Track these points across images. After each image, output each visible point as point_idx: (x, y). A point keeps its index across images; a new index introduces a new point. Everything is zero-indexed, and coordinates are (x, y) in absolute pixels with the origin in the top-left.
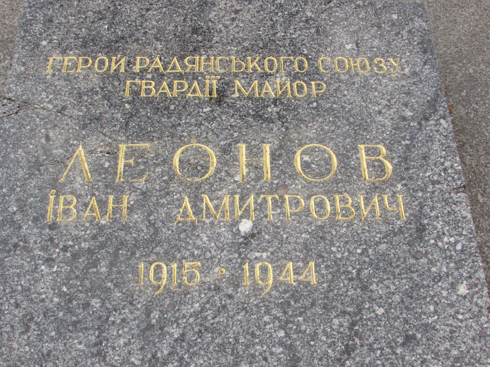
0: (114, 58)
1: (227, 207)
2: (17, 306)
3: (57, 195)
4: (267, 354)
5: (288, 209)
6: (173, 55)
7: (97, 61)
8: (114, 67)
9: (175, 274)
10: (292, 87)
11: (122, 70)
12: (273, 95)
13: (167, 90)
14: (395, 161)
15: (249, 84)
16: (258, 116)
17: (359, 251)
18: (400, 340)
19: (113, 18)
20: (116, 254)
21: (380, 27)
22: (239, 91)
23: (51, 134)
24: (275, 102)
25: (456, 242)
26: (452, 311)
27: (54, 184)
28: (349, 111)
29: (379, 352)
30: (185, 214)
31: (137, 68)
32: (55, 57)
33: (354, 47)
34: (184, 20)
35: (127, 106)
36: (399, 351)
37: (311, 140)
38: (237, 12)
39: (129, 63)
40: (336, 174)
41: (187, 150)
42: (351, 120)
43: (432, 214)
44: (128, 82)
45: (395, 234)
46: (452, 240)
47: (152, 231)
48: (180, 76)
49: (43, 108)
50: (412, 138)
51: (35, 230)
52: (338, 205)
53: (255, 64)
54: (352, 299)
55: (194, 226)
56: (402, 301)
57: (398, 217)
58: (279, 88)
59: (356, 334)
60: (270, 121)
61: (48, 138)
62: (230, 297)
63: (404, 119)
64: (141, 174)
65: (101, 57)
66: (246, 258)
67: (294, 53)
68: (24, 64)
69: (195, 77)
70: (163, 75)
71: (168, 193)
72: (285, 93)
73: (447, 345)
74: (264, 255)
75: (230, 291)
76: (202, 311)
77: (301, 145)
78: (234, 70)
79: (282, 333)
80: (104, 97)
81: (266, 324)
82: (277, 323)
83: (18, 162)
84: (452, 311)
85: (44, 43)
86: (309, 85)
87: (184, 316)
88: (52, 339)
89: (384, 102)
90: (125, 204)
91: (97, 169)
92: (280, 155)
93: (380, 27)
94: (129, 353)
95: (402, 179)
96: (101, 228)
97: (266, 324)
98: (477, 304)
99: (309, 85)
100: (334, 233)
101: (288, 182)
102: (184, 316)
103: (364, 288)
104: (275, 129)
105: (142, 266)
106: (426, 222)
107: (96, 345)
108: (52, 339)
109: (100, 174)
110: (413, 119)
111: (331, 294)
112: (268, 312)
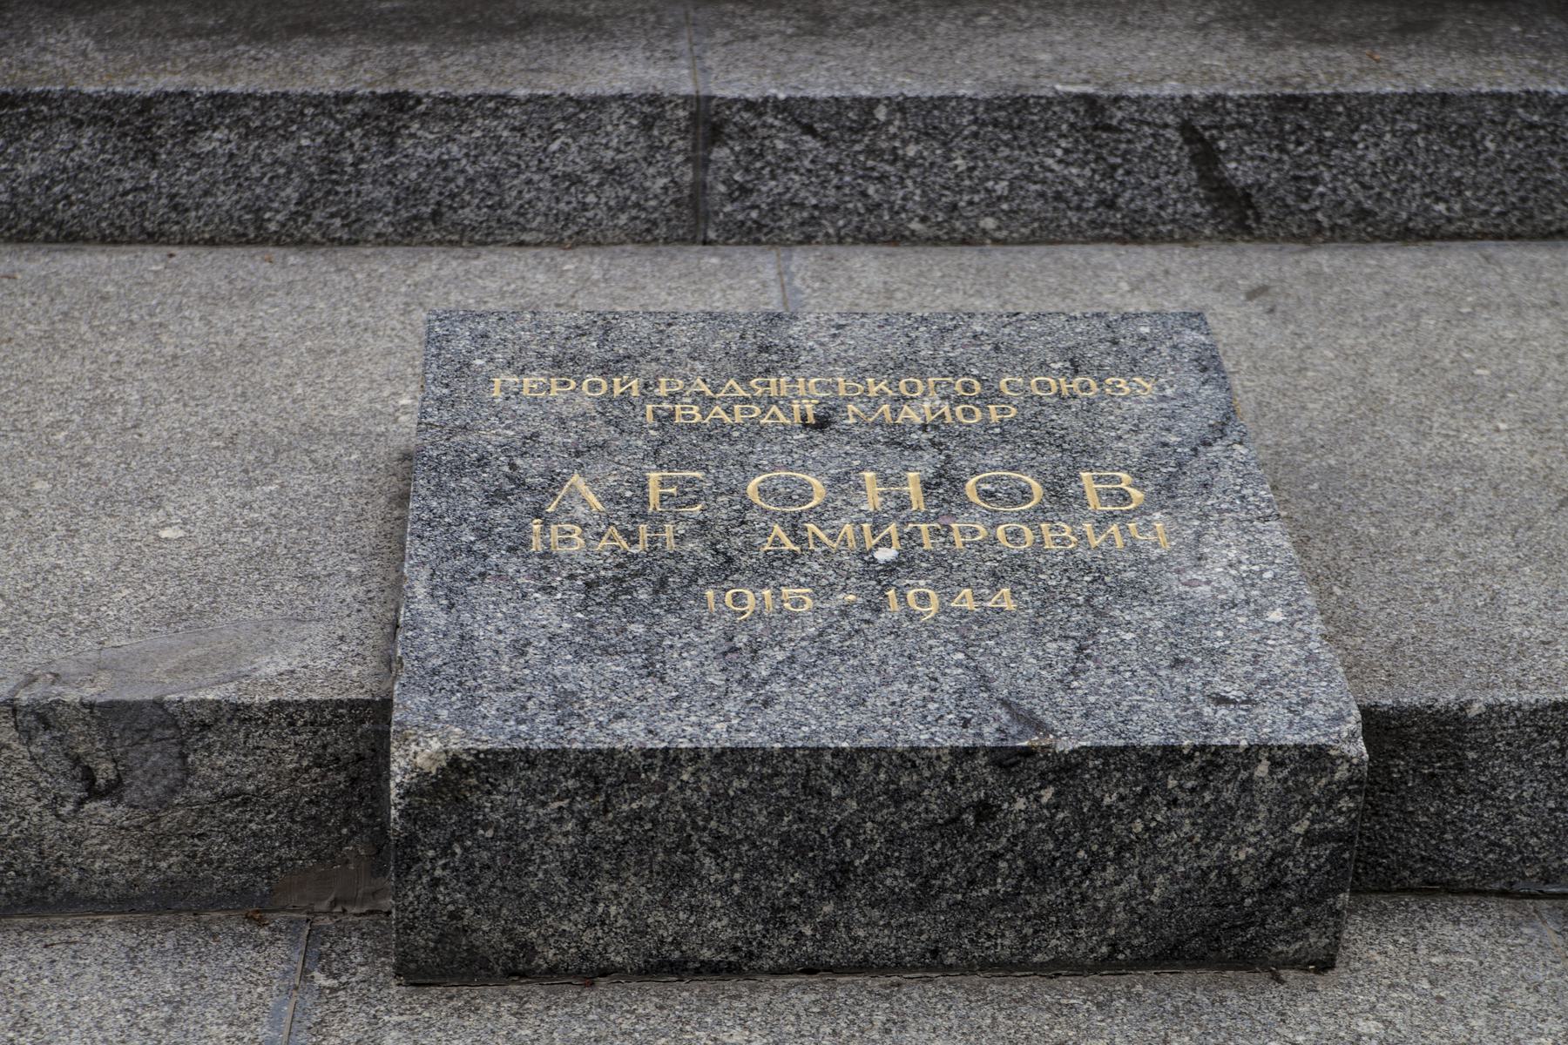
0: (616, 380)
1: (850, 536)
2: (500, 632)
3: (546, 524)
4: (938, 675)
5: (959, 541)
6: (728, 377)
7: (585, 383)
8: (618, 391)
9: (769, 602)
10: (953, 413)
11: (635, 393)
12: (919, 421)
13: (723, 415)
14: (1150, 489)
15: (874, 409)
16: (891, 443)
17: (1087, 578)
18: (1165, 663)
19: (606, 333)
20: (663, 583)
21: (1115, 342)
22: (856, 416)
23: (519, 462)
24: (924, 428)
25: (1262, 572)
26: (1257, 637)
27: (538, 513)
28: (1062, 437)
29: (1128, 674)
30: (776, 542)
31: (662, 391)
32: (504, 380)
33: (1068, 364)
34: (742, 337)
35: (652, 432)
36: (1163, 673)
37: (995, 468)
38: (840, 327)
39: (646, 386)
40: (1041, 502)
41: (770, 479)
42: (1066, 446)
43: (1221, 542)
44: (649, 407)
45: (1152, 563)
46: (1256, 568)
47: (721, 559)
48: (746, 400)
49: (497, 434)
50: (1179, 465)
51: (514, 559)
52: (1048, 536)
53: (881, 385)
54: (1079, 625)
55: (795, 555)
56: (1167, 627)
57: (1156, 545)
58: (928, 413)
59: (1088, 656)
60: (916, 448)
61: (513, 466)
62: (868, 622)
63: (1165, 445)
64: (695, 502)
65: (590, 378)
66: (889, 584)
67: (955, 374)
68: (447, 386)
69: (772, 401)
70: (712, 399)
71: (743, 523)
72: (942, 416)
73: (1249, 668)
74: (922, 582)
75: (867, 616)
76: (820, 635)
77: (976, 473)
78: (842, 393)
79: (960, 656)
80: (609, 422)
81: (931, 647)
82: (950, 646)
83: (465, 491)
84: (1257, 637)
85: (478, 362)
86: (984, 409)
87: (791, 640)
88: (568, 662)
89: (1126, 427)
90: (669, 534)
91: (612, 498)
92: (938, 485)
93: (1115, 342)
94: (703, 674)
95: (1162, 507)
96: (634, 557)
97: (931, 647)
98: (1300, 631)
99: (984, 409)
100: (1041, 560)
101: (954, 511)
102: (791, 640)
103: (1099, 614)
104: (927, 457)
105: (710, 593)
106: (1206, 550)
107: (645, 667)
108: (568, 662)
109: (618, 503)
110: (1181, 444)
111: (1041, 620)
112: (934, 635)
